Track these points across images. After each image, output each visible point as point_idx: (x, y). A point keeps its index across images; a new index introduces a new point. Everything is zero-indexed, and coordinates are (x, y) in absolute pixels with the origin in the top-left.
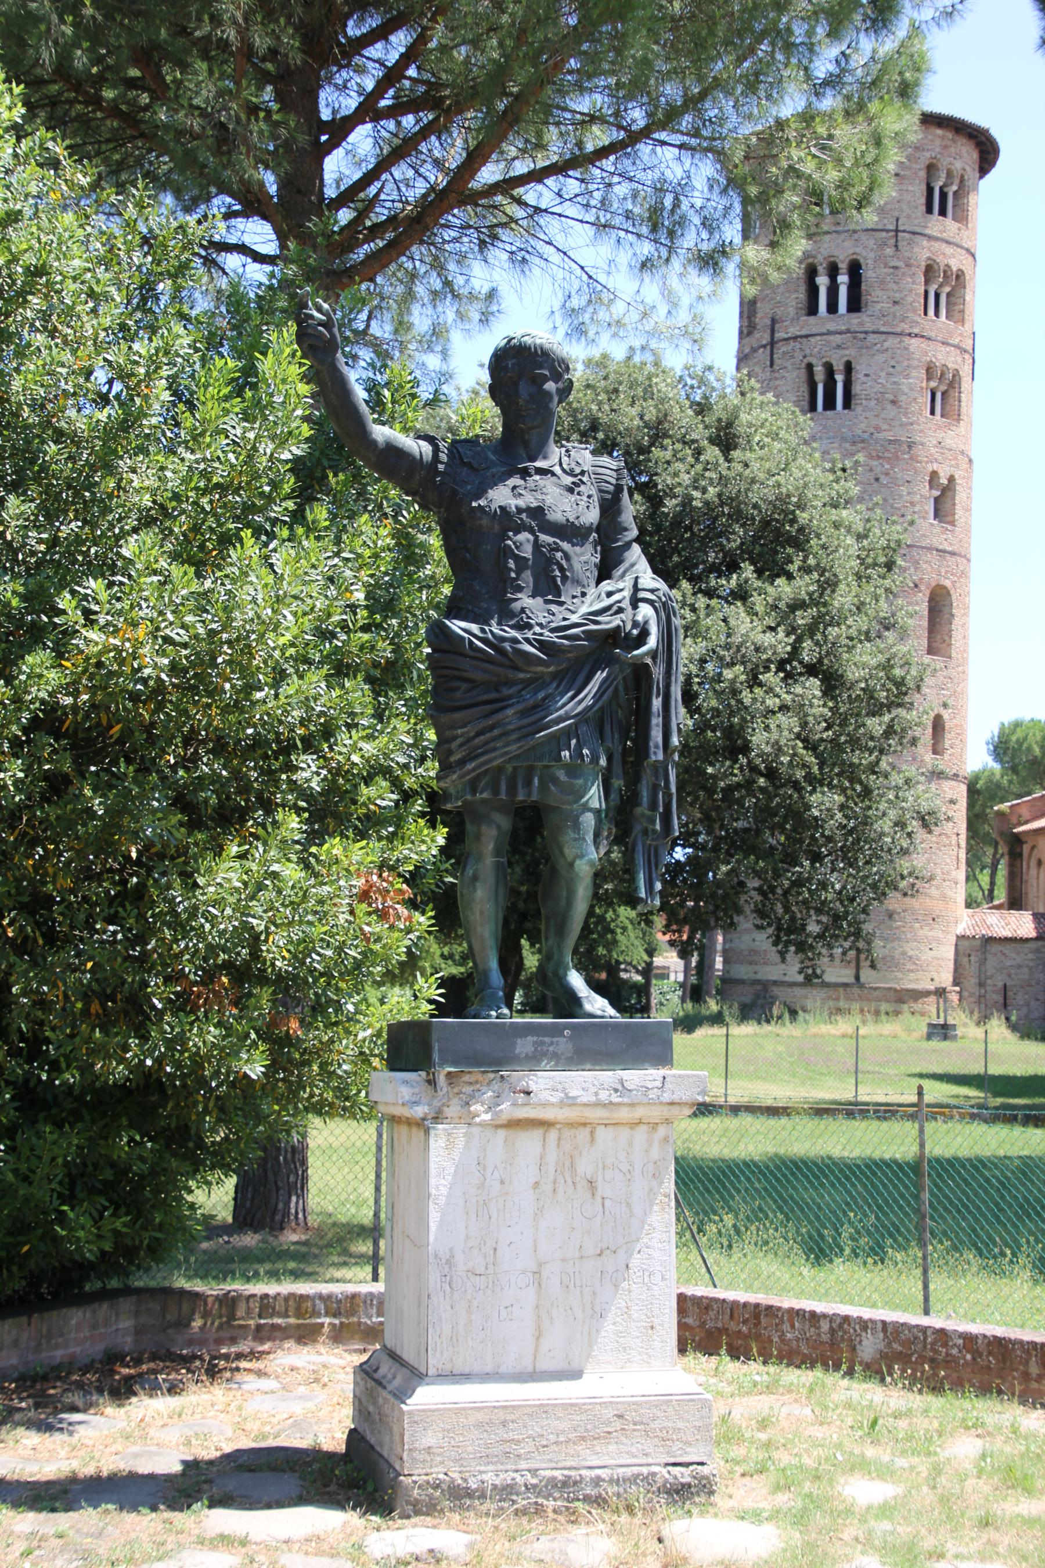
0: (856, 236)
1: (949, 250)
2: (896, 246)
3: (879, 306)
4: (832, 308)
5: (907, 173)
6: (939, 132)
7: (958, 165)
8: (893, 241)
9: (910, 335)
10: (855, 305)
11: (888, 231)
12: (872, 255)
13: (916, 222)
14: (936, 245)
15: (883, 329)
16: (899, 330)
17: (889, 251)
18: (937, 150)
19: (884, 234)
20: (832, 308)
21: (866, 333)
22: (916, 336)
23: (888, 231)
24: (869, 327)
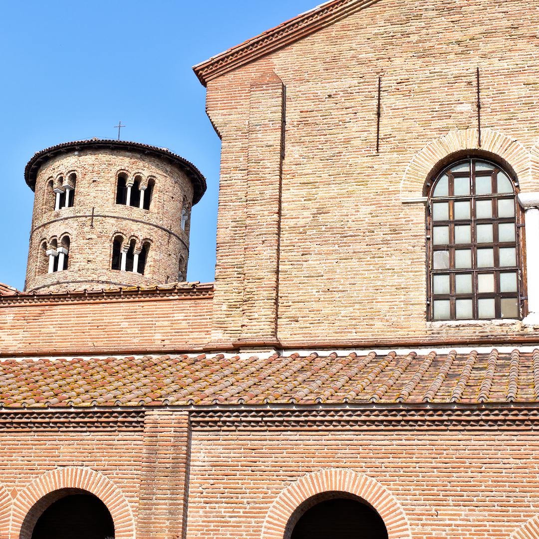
0: (67, 221)
1: (135, 226)
2: (92, 225)
3: (77, 265)
4: (55, 269)
5: (103, 180)
6: (128, 154)
7: (145, 174)
8: (89, 223)
9: (98, 282)
10: (65, 267)
11: (86, 217)
12: (75, 232)
13: (107, 209)
14: (125, 222)
15: (79, 279)
16: (90, 279)
17: (87, 229)
18: (126, 165)
19: (84, 219)
20: (55, 269)
21: (68, 283)
22: (103, 282)
23: (86, 217)
24: (70, 279)
